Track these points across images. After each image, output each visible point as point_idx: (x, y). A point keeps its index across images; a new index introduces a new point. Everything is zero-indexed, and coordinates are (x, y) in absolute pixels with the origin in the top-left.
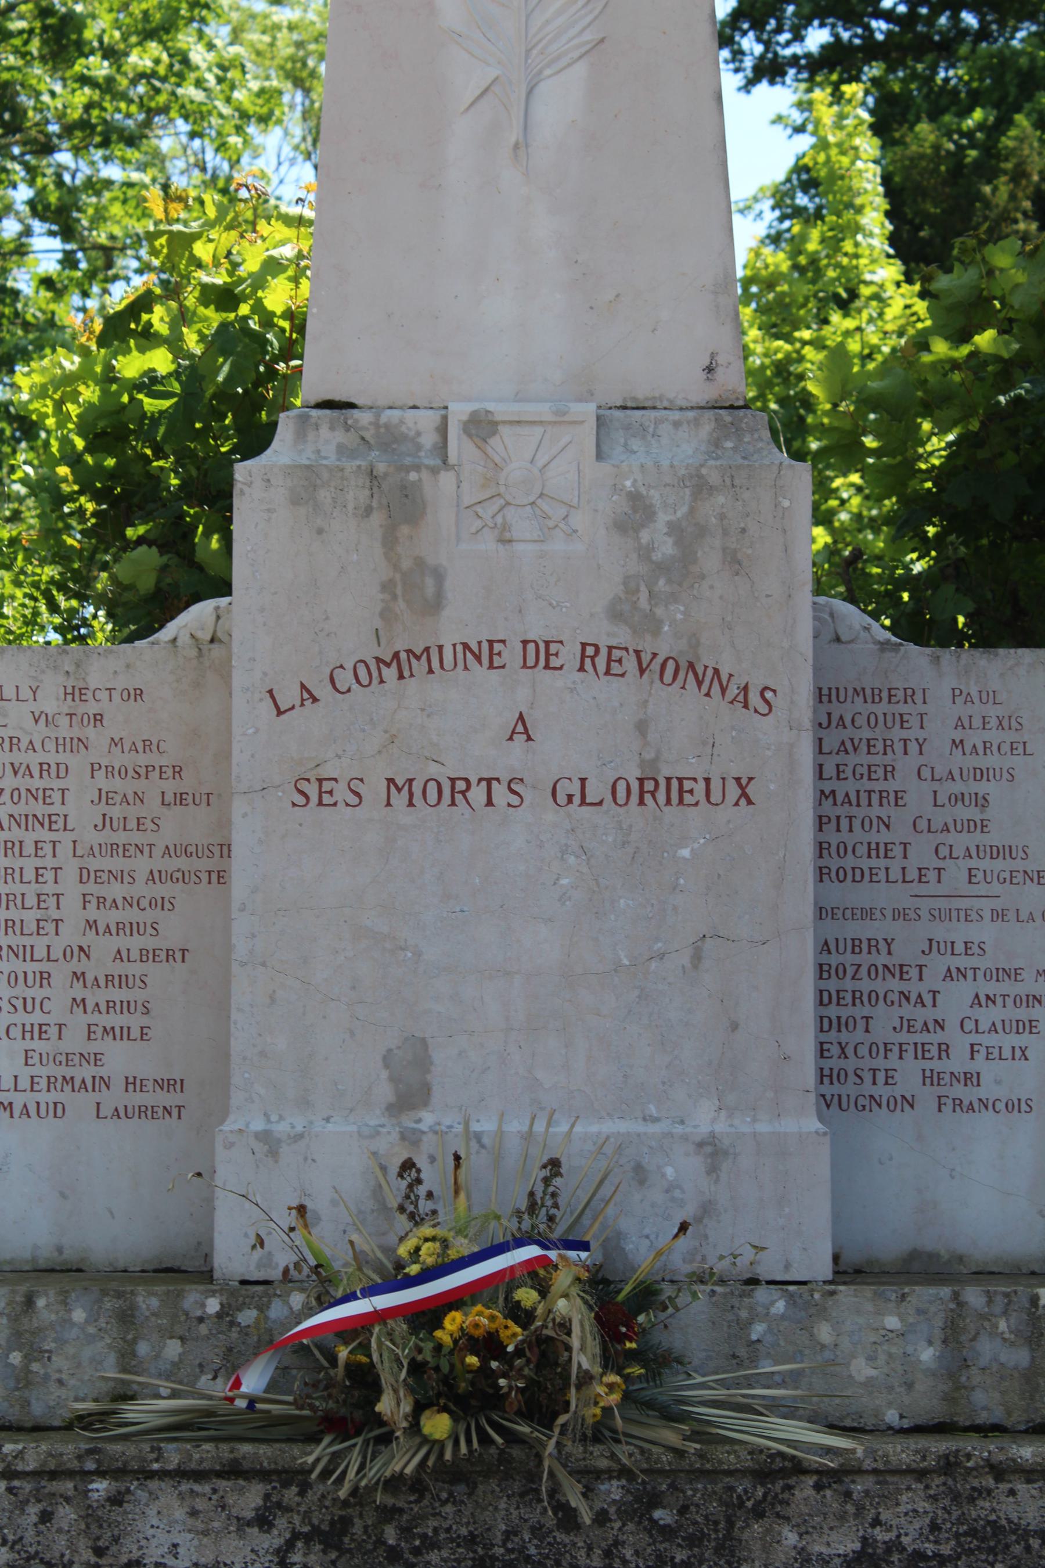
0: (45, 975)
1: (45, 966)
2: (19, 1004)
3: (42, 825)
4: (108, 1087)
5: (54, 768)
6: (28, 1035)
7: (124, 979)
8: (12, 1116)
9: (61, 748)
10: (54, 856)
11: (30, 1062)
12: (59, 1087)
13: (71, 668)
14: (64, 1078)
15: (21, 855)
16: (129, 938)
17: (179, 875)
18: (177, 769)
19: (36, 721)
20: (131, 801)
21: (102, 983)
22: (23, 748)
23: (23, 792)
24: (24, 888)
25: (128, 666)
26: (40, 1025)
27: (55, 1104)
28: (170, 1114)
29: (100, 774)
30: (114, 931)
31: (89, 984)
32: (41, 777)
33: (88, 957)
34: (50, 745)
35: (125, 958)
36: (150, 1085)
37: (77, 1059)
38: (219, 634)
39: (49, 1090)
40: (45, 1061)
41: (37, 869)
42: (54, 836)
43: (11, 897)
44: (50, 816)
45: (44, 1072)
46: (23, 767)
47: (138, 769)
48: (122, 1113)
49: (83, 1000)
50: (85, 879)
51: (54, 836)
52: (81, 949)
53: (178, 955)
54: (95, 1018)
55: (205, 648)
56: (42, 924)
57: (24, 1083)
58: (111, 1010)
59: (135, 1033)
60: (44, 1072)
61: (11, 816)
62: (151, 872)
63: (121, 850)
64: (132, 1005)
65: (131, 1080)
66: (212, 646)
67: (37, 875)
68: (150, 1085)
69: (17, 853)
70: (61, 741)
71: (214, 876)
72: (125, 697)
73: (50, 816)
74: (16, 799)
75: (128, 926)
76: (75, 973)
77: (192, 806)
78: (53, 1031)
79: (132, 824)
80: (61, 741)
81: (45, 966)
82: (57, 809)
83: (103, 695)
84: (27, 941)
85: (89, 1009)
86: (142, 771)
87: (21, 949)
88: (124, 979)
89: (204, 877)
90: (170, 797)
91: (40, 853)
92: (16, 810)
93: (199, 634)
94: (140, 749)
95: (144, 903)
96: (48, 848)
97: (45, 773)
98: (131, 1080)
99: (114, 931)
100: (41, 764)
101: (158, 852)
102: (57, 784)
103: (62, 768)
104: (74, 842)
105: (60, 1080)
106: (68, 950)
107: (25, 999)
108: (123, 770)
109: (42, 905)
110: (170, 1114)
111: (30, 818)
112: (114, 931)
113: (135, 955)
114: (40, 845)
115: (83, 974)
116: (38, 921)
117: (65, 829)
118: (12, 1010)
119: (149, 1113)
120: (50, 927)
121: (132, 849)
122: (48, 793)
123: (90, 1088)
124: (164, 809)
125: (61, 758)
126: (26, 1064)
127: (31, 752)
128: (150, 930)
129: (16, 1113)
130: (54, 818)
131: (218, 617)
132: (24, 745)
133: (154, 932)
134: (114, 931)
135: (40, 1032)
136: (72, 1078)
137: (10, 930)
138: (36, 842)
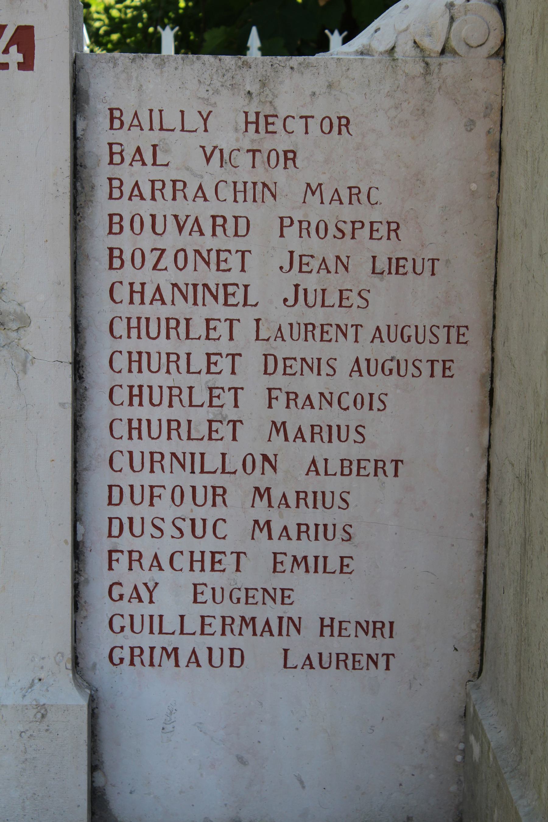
0: (219, 491)
1: (219, 480)
2: (186, 527)
3: (216, 298)
4: (299, 631)
5: (231, 222)
6: (197, 566)
7: (319, 497)
8: (177, 665)
9: (240, 197)
10: (231, 339)
11: (200, 598)
12: (236, 630)
13: (255, 88)
14: (243, 618)
15: (188, 337)
16: (326, 445)
17: (393, 365)
18: (393, 226)
19: (208, 160)
20: (332, 269)
21: (292, 501)
22: (190, 196)
23: (191, 255)
24: (191, 380)
25: (330, 86)
26: (213, 554)
27: (232, 650)
28: (376, 664)
29: (292, 232)
30: (307, 436)
31: (275, 503)
32: (214, 234)
33: (274, 468)
34: (226, 192)
35: (322, 470)
36: (351, 628)
37: (259, 595)
38: (453, 43)
39: (223, 634)
40: (218, 598)
41: (208, 355)
42: (230, 312)
43: (176, 392)
44: (225, 286)
45: (218, 610)
46: (191, 221)
47: (341, 225)
48: (316, 663)
49: (268, 523)
50: (270, 369)
51: (230, 312)
52: (265, 458)
53: (390, 468)
54: (282, 545)
55: (434, 62)
56: (215, 426)
57: (192, 625)
58: (303, 536)
59: (334, 564)
60: (218, 610)
61: (175, 285)
62: (357, 361)
63: (318, 332)
64: (330, 529)
65: (327, 622)
66: (444, 59)
67: (209, 363)
68: (351, 628)
69: (183, 335)
70: (240, 187)
71: (438, 368)
72: (326, 129)
73: (225, 286)
74: (181, 264)
75: (326, 430)
76: (257, 489)
77: (411, 275)
78: (229, 561)
79: (333, 298)
80: (240, 187)
81: (219, 480)
82: (234, 276)
83: (297, 125)
84: (196, 447)
85: (276, 533)
86: (348, 229)
87: (188, 457)
88: (319, 497)
89: (426, 368)
90: (383, 263)
91: (212, 334)
92: (181, 278)
93: (426, 43)
94: (346, 200)
95: (347, 401)
96: (223, 329)
97: (219, 230)
98: (327, 622)
99: (308, 436)
100: (214, 217)
101: (366, 334)
102: (235, 244)
103: (242, 222)
104: (258, 321)
105: (238, 621)
106: (249, 459)
107: (193, 521)
108: (322, 226)
109: (216, 402)
110: (376, 664)
111: (200, 289)
112: (308, 436)
113: (334, 466)
114: (212, 324)
115: (268, 489)
116: (210, 422)
117: (245, 304)
118: (177, 534)
119: (350, 662)
120: (226, 430)
121: (333, 331)
122: (223, 256)
123: (275, 631)
124: (376, 279)
125: (241, 209)
126: (195, 601)
127: (200, 201)
128: (353, 435)
129: (183, 661)
130: (230, 289)
131: (452, 19)
132: (191, 191)
133: (360, 439)
134: (307, 436)
135: (213, 563)
136: (253, 619)
137: (174, 434)
138: (208, 321)
